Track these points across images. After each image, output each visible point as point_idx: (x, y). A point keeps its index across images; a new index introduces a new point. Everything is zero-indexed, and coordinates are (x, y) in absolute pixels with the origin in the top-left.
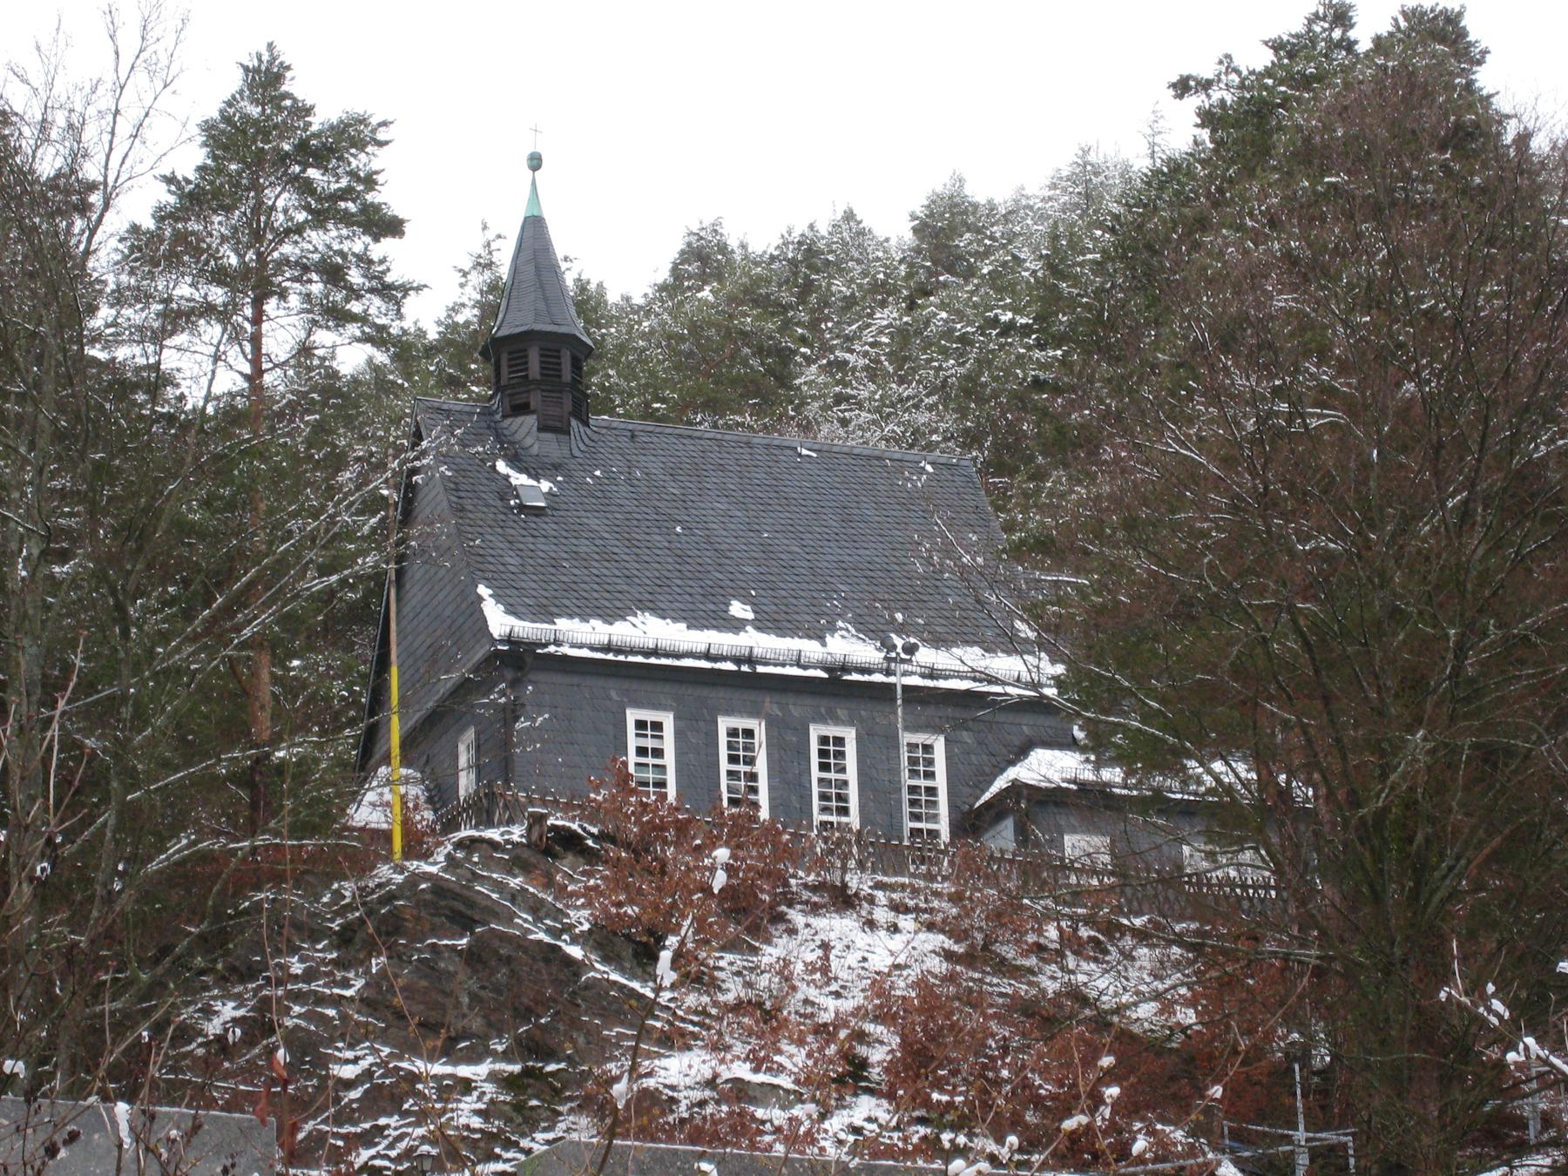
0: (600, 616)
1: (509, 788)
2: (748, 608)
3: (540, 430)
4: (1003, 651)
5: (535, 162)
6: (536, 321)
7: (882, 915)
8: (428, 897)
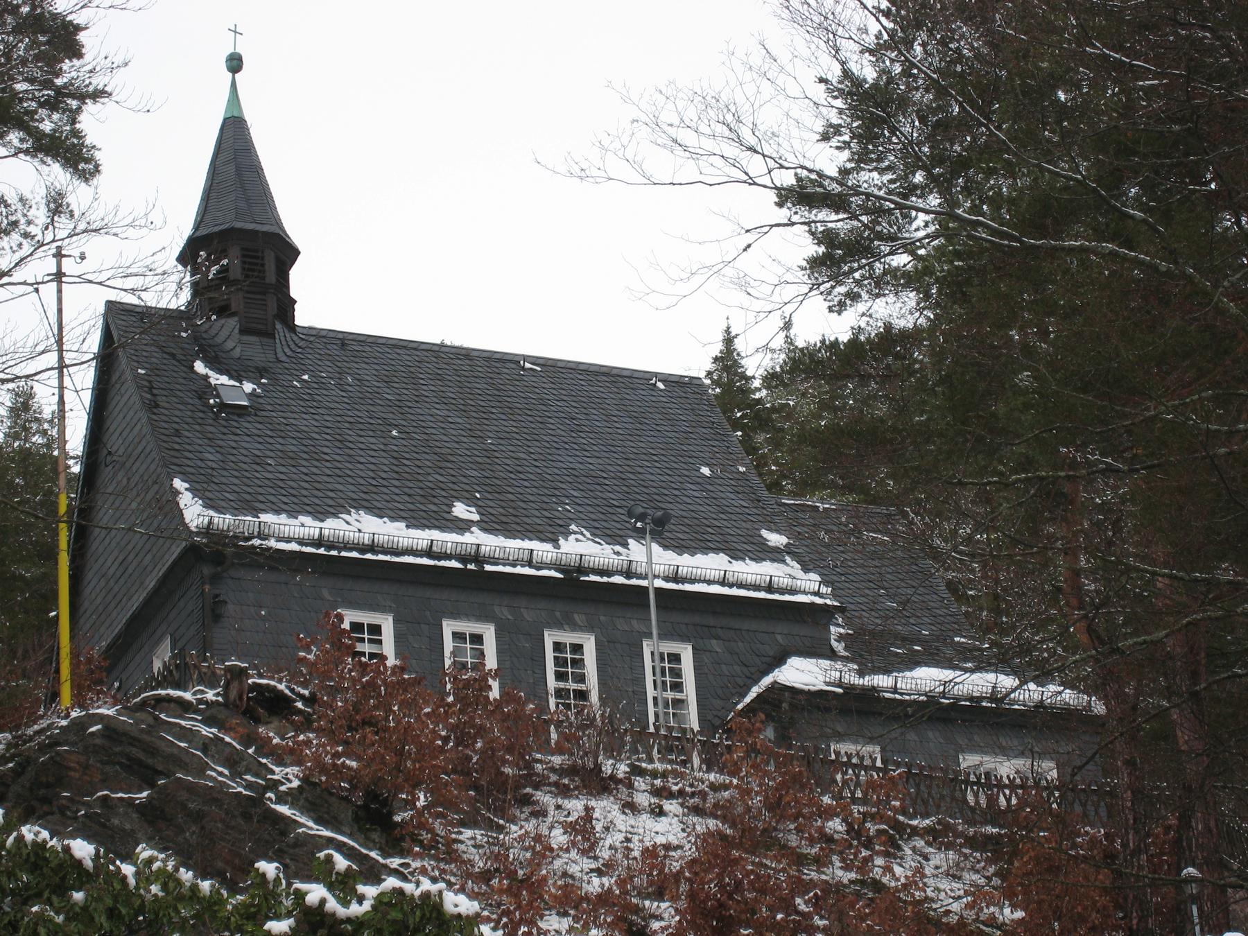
0: (309, 513)
1: (205, 660)
2: (473, 509)
3: (242, 332)
4: (751, 559)
5: (235, 63)
6: (238, 217)
7: (643, 799)
8: (98, 741)
